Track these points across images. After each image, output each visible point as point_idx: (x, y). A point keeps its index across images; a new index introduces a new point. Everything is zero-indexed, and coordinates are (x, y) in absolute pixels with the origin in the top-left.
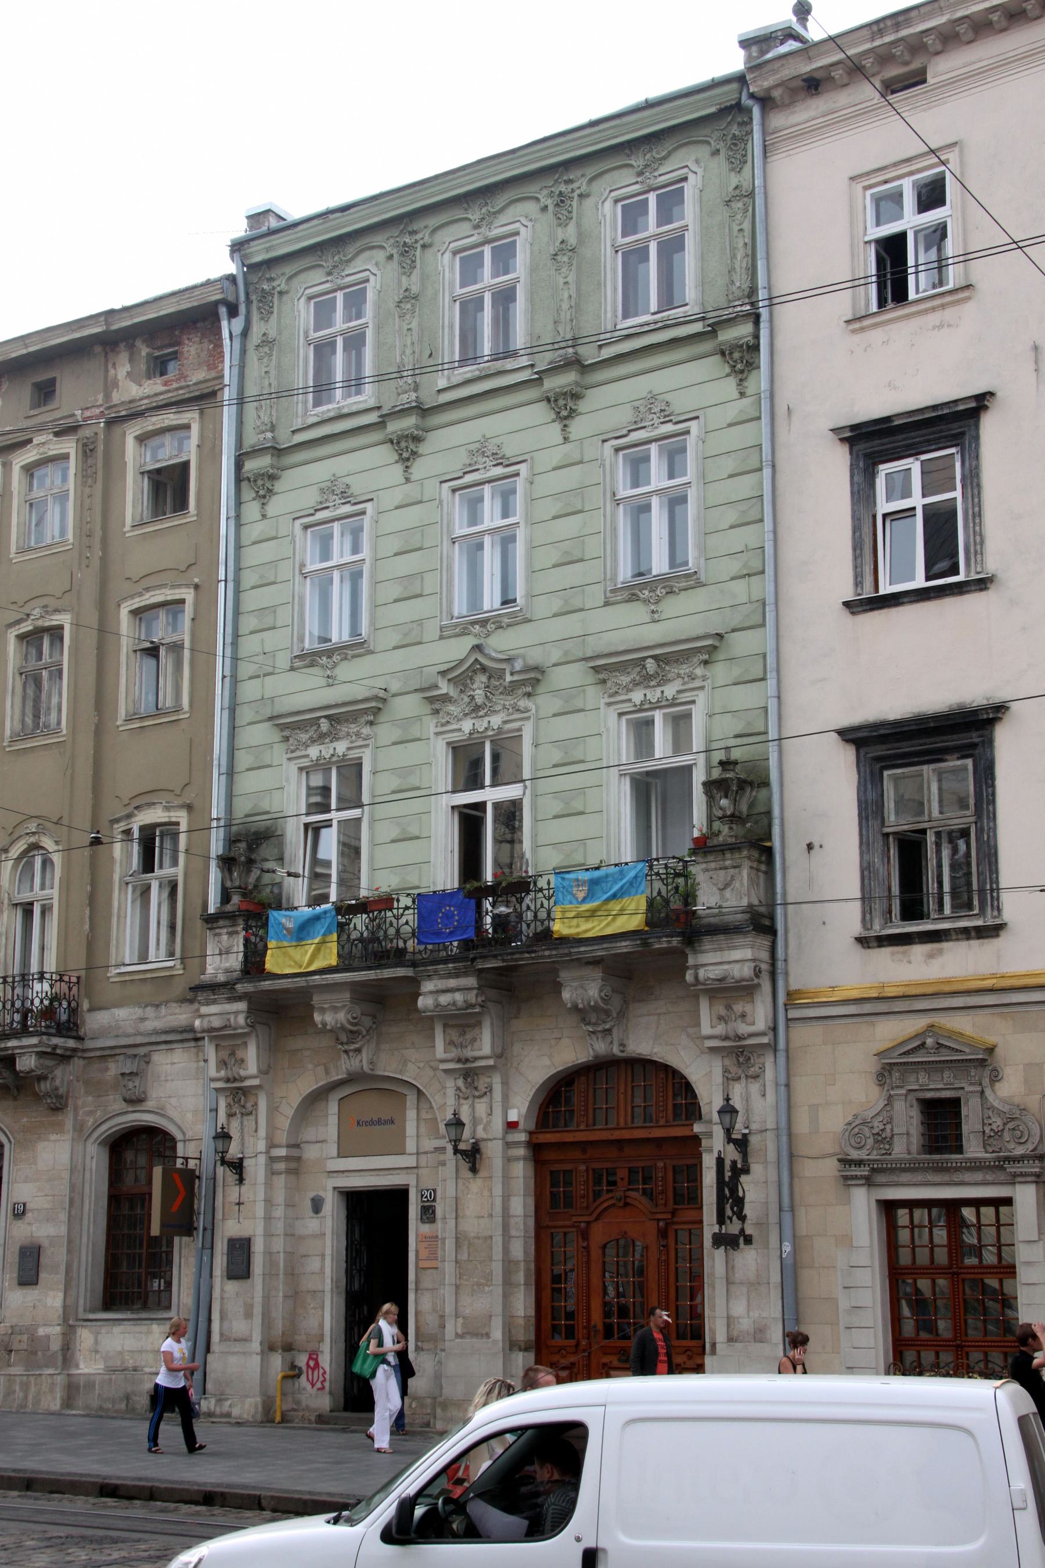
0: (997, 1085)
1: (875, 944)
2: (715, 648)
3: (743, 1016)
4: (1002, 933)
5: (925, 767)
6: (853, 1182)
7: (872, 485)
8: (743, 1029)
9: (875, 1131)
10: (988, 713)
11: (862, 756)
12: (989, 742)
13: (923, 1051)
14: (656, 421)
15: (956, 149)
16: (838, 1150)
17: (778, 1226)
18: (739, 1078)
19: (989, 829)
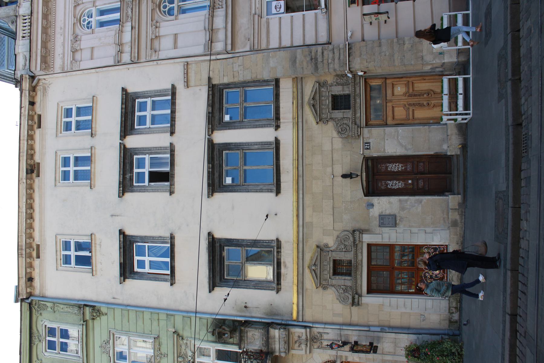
0: (329, 246)
1: (280, 286)
2: (178, 335)
3: (299, 337)
4: (280, 239)
5: (225, 263)
6: (360, 301)
7: (139, 272)
8: (304, 337)
9: (343, 291)
10: (210, 238)
11: (220, 285)
12: (220, 240)
13: (316, 270)
14: (108, 346)
15: (57, 236)
16: (349, 307)
17: (375, 333)
18: (321, 342)
19: (247, 242)
